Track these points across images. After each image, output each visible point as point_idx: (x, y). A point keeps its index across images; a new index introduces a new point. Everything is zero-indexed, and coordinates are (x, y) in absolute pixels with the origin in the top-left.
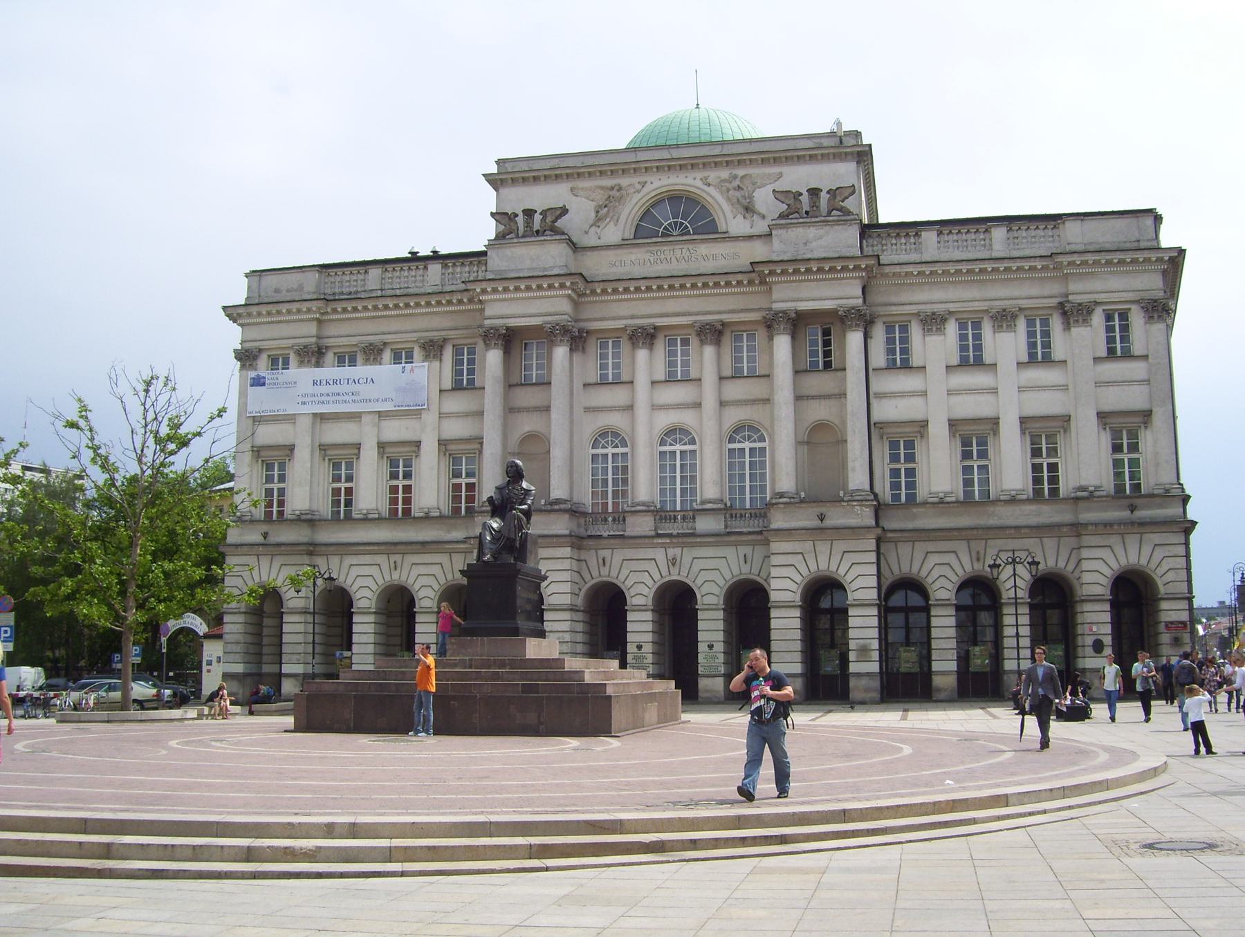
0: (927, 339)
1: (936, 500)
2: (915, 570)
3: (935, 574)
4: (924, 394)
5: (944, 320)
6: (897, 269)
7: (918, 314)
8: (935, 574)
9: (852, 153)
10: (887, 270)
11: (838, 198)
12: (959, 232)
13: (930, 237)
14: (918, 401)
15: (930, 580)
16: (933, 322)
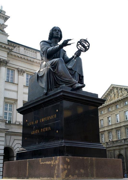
0: (19, 76)
1: (18, 124)
2: (10, 145)
3: (16, 147)
4: (17, 92)
5: (24, 72)
6: (15, 54)
7: (18, 69)
8: (16, 147)
9: (3, 17)
10: (12, 53)
11: (2, 27)
12: (31, 51)
13: (22, 49)
14: (15, 94)
15: (15, 148)
16: (21, 72)
